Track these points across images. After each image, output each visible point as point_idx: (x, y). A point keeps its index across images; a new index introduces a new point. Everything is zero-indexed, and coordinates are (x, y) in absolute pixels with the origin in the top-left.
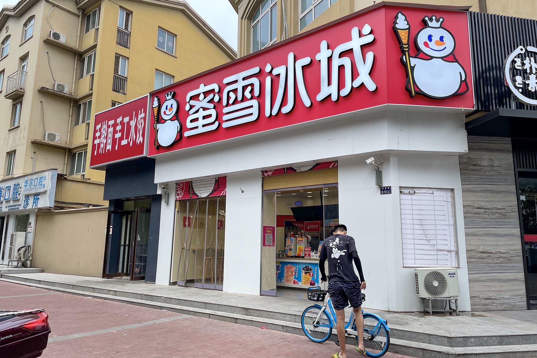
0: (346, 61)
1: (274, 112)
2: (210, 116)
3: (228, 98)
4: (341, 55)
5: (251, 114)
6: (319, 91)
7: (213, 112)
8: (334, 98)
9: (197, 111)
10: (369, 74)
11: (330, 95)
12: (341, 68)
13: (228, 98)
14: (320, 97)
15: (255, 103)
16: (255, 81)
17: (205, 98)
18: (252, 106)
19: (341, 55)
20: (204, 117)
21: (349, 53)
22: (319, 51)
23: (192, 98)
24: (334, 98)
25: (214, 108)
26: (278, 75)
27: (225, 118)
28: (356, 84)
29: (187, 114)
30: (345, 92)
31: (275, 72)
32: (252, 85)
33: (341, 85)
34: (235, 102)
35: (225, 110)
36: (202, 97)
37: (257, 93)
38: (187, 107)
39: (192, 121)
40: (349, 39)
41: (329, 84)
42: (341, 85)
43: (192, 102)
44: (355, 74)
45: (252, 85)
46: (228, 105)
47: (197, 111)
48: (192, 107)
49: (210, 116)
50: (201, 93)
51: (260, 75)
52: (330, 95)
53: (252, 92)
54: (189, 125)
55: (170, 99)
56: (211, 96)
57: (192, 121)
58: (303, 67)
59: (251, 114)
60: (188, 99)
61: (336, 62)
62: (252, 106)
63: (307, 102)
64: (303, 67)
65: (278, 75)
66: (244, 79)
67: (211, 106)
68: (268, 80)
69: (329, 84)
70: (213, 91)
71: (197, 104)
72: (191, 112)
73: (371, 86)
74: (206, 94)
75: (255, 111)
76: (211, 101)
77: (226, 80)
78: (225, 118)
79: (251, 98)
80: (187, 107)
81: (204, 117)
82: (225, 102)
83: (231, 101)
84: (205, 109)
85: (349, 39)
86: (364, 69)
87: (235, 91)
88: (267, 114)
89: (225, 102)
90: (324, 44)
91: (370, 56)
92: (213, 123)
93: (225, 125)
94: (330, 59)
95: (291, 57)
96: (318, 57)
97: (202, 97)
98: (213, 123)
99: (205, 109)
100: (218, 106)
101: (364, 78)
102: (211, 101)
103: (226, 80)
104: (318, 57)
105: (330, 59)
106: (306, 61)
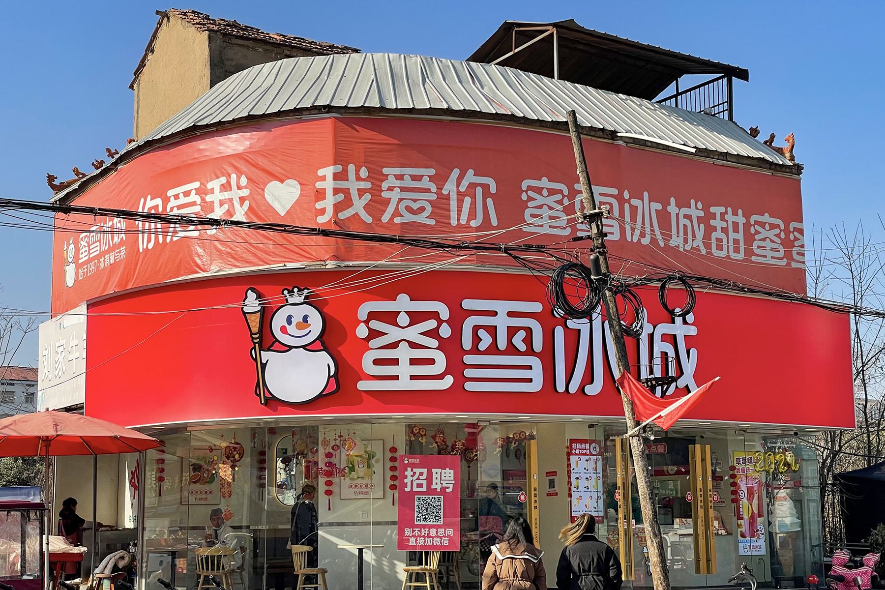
2: (431, 362)
3: (477, 339)
5: (531, 380)
9: (394, 345)
13: (477, 339)
15: (535, 362)
18: (530, 367)
20: (413, 362)
23: (373, 315)
27: (468, 373)
34: (493, 349)
35: (468, 359)
36: (403, 319)
37: (538, 346)
38: (362, 331)
39: (377, 362)
43: (375, 325)
45: (529, 331)
46: (475, 350)
47: (394, 345)
48: (374, 334)
49: (431, 362)
50: (401, 312)
53: (528, 340)
54: (368, 365)
56: (432, 324)
57: (377, 362)
59: (531, 380)
62: (530, 367)
66: (511, 314)
67: (435, 343)
70: (435, 315)
71: (393, 333)
75: (537, 373)
78: (468, 373)
80: (362, 331)
81: (413, 362)
82: (467, 344)
83: (482, 346)
84: (413, 345)
89: (467, 344)
92: (440, 377)
93: (469, 386)
97: (403, 319)
99: (413, 345)
102: (432, 334)
103: (468, 304)
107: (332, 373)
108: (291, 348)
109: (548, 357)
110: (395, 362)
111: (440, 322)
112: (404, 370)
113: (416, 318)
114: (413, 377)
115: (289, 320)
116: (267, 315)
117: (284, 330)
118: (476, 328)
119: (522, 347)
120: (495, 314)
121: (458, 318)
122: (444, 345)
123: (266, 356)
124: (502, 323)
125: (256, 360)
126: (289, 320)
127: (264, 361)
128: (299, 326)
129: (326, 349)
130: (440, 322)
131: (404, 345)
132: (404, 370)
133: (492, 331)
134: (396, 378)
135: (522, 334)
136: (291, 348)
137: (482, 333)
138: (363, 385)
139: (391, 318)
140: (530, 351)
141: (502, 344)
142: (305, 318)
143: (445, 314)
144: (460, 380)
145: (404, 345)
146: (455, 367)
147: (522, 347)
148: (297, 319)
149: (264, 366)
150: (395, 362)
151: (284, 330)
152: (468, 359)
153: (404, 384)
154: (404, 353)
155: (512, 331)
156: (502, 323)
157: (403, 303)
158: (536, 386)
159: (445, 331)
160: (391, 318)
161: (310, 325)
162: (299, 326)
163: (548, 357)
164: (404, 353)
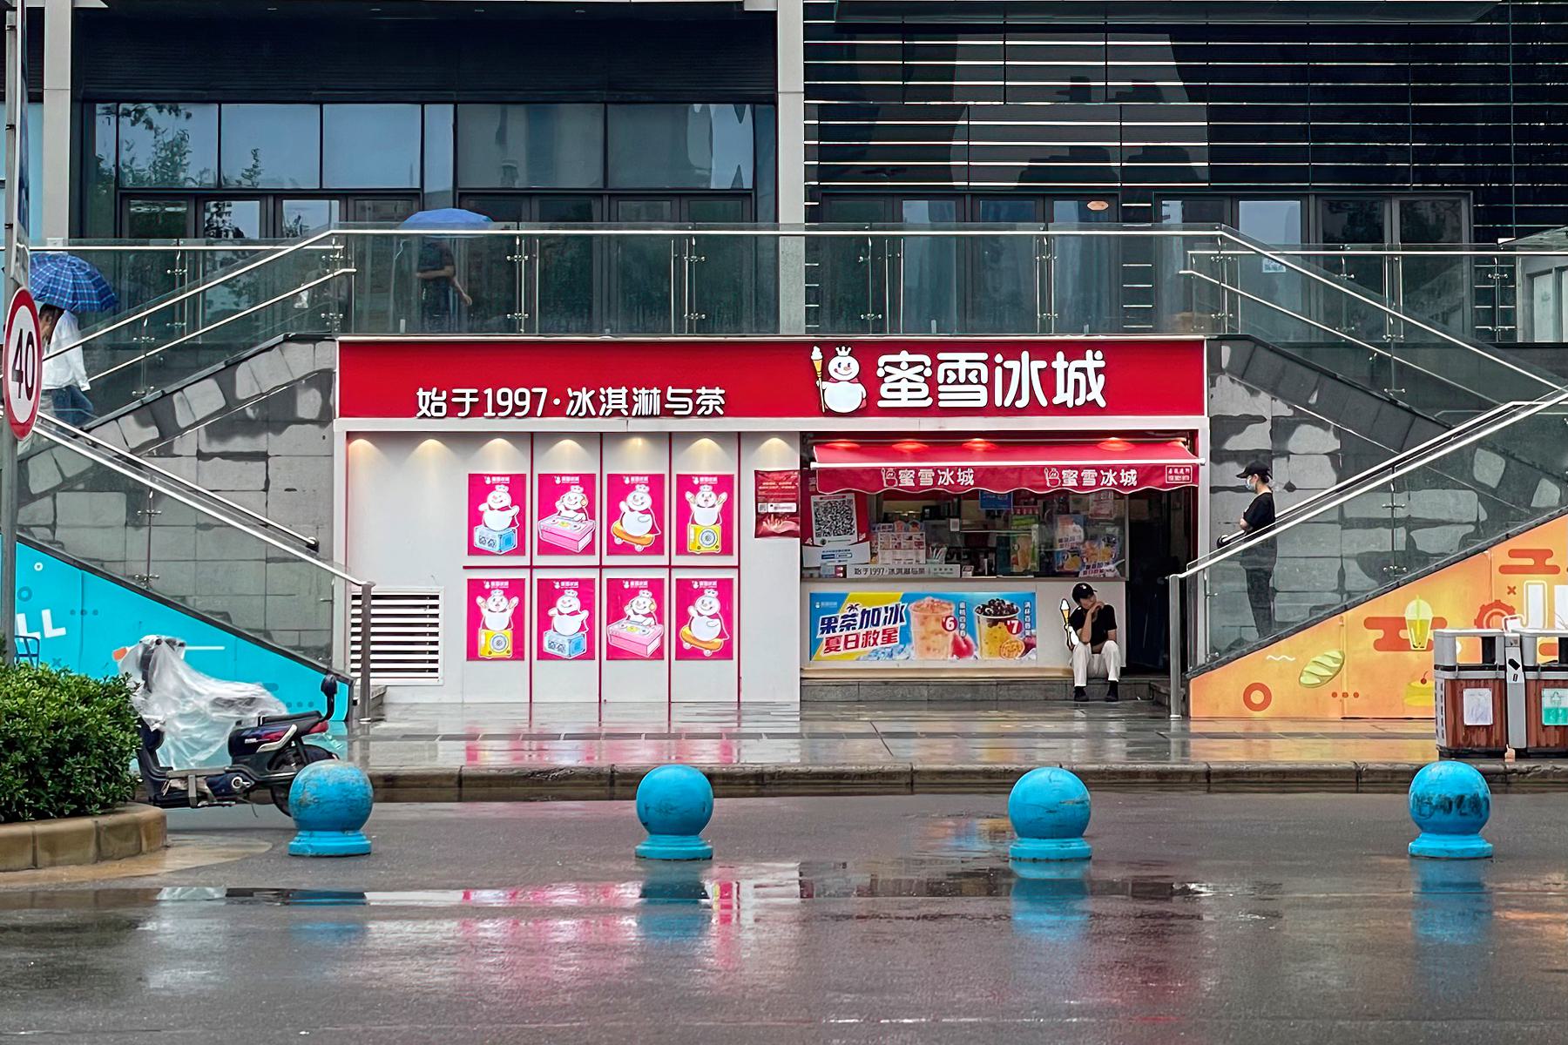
0: (1081, 376)
1: (1008, 403)
2: (919, 390)
3: (946, 377)
4: (1077, 370)
7: (925, 390)
8: (1070, 405)
9: (899, 381)
12: (1077, 382)
13: (946, 377)
14: (1056, 401)
19: (1077, 370)
20: (910, 390)
21: (1084, 370)
23: (887, 364)
26: (1011, 370)
28: (1090, 398)
29: (882, 380)
30: (1080, 402)
31: (1008, 364)
33: (1076, 395)
34: (957, 382)
36: (904, 366)
37: (984, 379)
39: (889, 390)
41: (1066, 391)
42: (1076, 395)
43: (888, 369)
44: (1089, 390)
45: (979, 371)
46: (945, 383)
47: (899, 381)
48: (888, 374)
49: (919, 390)
53: (979, 376)
56: (919, 368)
57: (889, 390)
58: (1039, 370)
61: (1072, 375)
63: (1044, 402)
65: (1011, 370)
68: (998, 371)
70: (922, 363)
71: (897, 373)
72: (886, 379)
73: (1102, 403)
74: (911, 365)
76: (921, 374)
80: (880, 373)
81: (910, 390)
82: (941, 379)
83: (949, 381)
84: (909, 381)
87: (956, 371)
88: (998, 403)
90: (1060, 355)
91: (1102, 378)
93: (941, 404)
94: (1066, 370)
96: (1054, 365)
97: (904, 366)
99: (909, 381)
100: (932, 382)
101: (1096, 395)
102: (921, 374)
103: (941, 356)
104: (1054, 365)
105: (1066, 370)
106: (1043, 364)
109: (990, 386)
110: (899, 390)
111: (925, 367)
112: (904, 395)
113: (911, 365)
117: (836, 370)
118: (946, 371)
119: (975, 381)
121: (936, 363)
122: (927, 380)
123: (824, 385)
124: (962, 366)
129: (860, 382)
130: (925, 367)
131: (904, 381)
132: (904, 395)
135: (976, 373)
137: (949, 373)
138: (881, 404)
139: (897, 365)
140: (980, 383)
141: (962, 379)
143: (928, 361)
144: (936, 400)
145: (904, 381)
146: (934, 393)
149: (824, 391)
150: (899, 390)
151: (836, 370)
154: (904, 385)
155: (968, 371)
156: (962, 366)
157: (904, 357)
158: (983, 403)
159: (928, 373)
160: (897, 365)
163: (990, 386)
164: (904, 385)
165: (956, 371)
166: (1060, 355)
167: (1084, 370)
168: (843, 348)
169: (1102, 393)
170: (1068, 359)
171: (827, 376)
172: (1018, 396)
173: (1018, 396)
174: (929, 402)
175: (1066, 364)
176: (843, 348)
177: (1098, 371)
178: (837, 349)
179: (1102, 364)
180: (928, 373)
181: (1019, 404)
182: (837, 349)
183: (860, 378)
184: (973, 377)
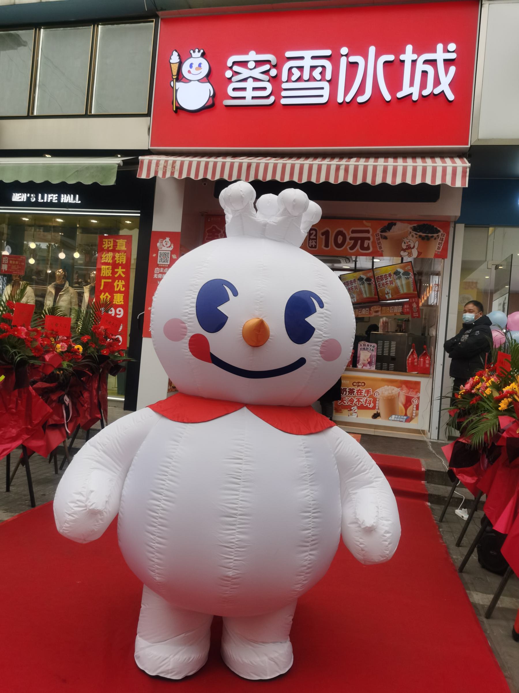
0: (429, 69)
1: (348, 99)
2: (264, 89)
4: (426, 62)
5: (322, 96)
6: (400, 89)
9: (245, 80)
10: (449, 85)
11: (411, 94)
12: (425, 73)
14: (400, 95)
15: (326, 85)
16: (327, 64)
17: (255, 68)
18: (322, 88)
19: (426, 62)
20: (255, 89)
21: (433, 62)
22: (404, 52)
23: (234, 63)
24: (415, 97)
25: (269, 81)
27: (284, 93)
28: (437, 91)
32: (324, 67)
34: (300, 79)
36: (251, 65)
37: (328, 76)
39: (234, 89)
40: (434, 51)
41: (412, 84)
43: (236, 68)
44: (437, 82)
46: (289, 80)
47: (245, 80)
49: (264, 89)
51: (334, 59)
52: (411, 94)
53: (322, 73)
55: (199, 57)
56: (267, 67)
57: (234, 89)
59: (322, 96)
60: (229, 64)
61: (420, 67)
62: (322, 88)
63: (388, 97)
64: (386, 63)
66: (313, 58)
67: (266, 77)
69: (412, 84)
70: (268, 62)
71: (245, 73)
72: (234, 79)
73: (451, 97)
74: (259, 63)
76: (266, 72)
77: (288, 54)
78: (284, 93)
79: (320, 80)
80: (228, 74)
81: (255, 89)
82: (284, 77)
83: (294, 78)
84: (255, 79)
85: (434, 51)
86: (446, 80)
88: (340, 100)
90: (409, 48)
91: (453, 69)
92: (268, 97)
93: (284, 101)
94: (414, 62)
95: (372, 50)
97: (251, 65)
98: (268, 97)
99: (255, 79)
100: (275, 80)
101: (445, 87)
103: (288, 54)
104: (402, 57)
105: (414, 62)
107: (211, 95)
108: (190, 81)
110: (244, 89)
113: (259, 63)
114: (253, 98)
115: (191, 66)
116: (181, 64)
117: (189, 72)
118: (290, 69)
119: (318, 77)
120: (302, 58)
124: (307, 63)
125: (173, 88)
126: (191, 66)
127: (177, 89)
128: (197, 69)
131: (250, 80)
133: (301, 68)
134: (244, 98)
135: (320, 69)
136: (190, 81)
137: (295, 71)
139: (244, 64)
140: (323, 79)
141: (306, 76)
142: (200, 65)
144: (279, 97)
145: (250, 80)
147: (318, 77)
148: (196, 65)
149: (176, 91)
150: (244, 89)
151: (189, 72)
152: (284, 86)
153: (249, 101)
154: (250, 84)
155: (313, 68)
156: (307, 63)
158: (324, 100)
160: (244, 64)
161: (202, 68)
162: (197, 69)
163: (333, 82)
164: (250, 84)
165: (301, 68)
166: (409, 48)
167: (433, 62)
168: (197, 50)
169: (450, 85)
170: (418, 51)
171: (180, 77)
172: (361, 91)
173: (361, 91)
174: (272, 99)
175: (415, 57)
176: (197, 50)
177: (448, 62)
178: (192, 52)
179: (453, 56)
180: (274, 72)
181: (361, 99)
182: (192, 52)
183: (208, 77)
184: (316, 74)
